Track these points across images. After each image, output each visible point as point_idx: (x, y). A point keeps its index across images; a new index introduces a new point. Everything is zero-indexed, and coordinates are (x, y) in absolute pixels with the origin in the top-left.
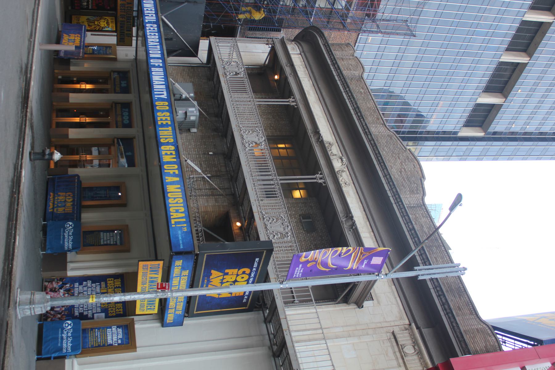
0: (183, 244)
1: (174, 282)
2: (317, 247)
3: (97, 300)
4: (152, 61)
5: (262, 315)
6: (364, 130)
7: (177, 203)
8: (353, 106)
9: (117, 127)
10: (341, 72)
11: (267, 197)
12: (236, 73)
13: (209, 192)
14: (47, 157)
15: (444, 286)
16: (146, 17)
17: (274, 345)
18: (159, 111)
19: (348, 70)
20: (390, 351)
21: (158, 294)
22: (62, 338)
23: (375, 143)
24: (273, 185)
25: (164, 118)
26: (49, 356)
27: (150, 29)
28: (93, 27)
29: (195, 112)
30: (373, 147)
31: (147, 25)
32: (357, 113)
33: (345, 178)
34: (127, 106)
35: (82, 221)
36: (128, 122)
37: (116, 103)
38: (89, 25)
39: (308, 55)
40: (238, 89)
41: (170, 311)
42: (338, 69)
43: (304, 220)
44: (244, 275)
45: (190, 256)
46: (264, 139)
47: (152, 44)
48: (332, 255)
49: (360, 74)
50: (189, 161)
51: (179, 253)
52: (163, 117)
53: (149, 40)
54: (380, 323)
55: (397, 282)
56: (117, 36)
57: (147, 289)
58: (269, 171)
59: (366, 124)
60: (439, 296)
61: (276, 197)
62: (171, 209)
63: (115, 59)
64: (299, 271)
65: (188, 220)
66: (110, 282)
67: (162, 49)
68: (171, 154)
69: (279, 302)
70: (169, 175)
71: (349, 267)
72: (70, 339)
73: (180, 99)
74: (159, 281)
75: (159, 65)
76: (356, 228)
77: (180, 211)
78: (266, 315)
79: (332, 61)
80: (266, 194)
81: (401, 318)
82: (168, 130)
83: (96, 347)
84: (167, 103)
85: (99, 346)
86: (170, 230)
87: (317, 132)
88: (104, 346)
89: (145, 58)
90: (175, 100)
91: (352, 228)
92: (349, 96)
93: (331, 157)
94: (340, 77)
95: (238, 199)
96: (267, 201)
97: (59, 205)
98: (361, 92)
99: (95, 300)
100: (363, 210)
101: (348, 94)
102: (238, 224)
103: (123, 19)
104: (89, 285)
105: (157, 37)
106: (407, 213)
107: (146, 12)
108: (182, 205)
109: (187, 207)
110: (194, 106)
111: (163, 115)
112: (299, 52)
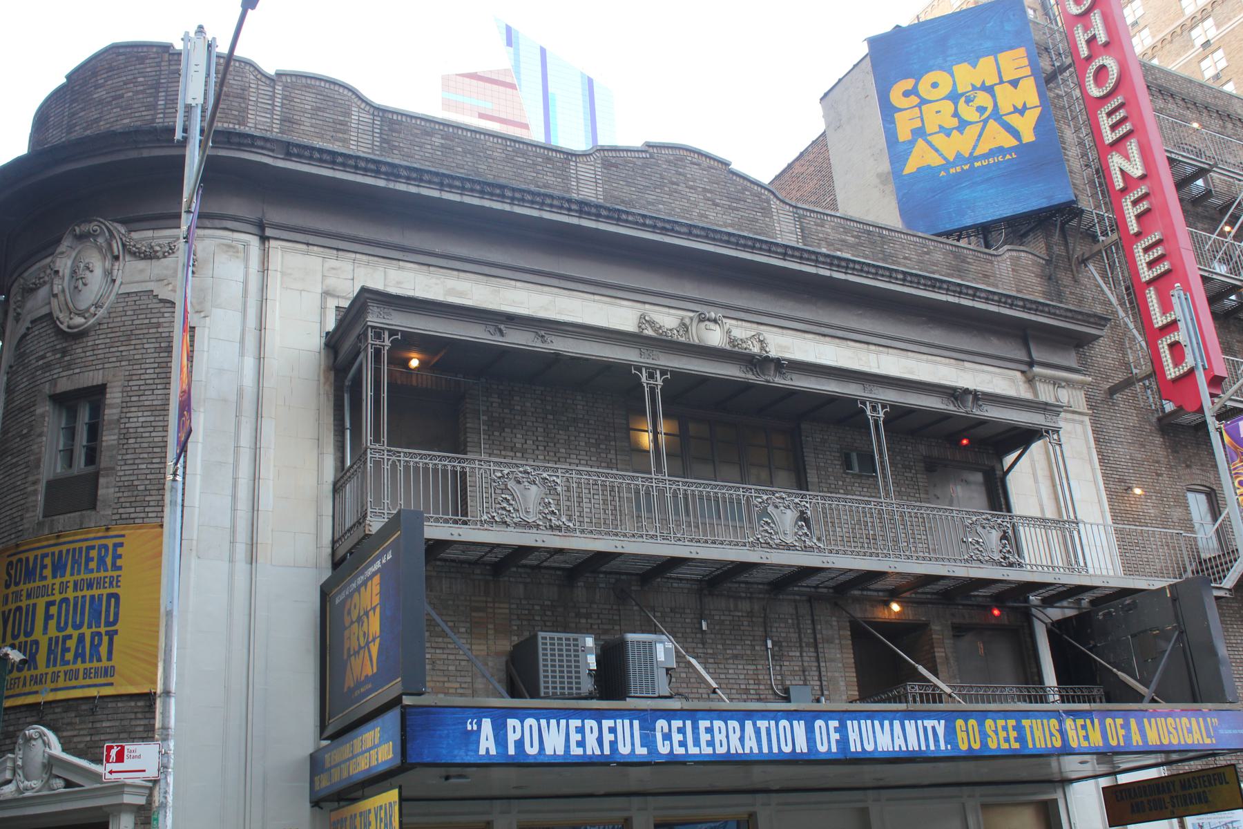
7: (1176, 729)
15: (952, 276)
18: (984, 744)
23: (703, 228)
25: (1002, 734)
30: (707, 237)
53: (735, 747)
60: (1012, 306)
67: (775, 715)
68: (1084, 727)
76: (984, 394)
79: (377, 173)
81: (1012, 380)
82: (1031, 727)
91: (978, 399)
106: (814, 253)
111: (992, 734)
112: (254, 241)
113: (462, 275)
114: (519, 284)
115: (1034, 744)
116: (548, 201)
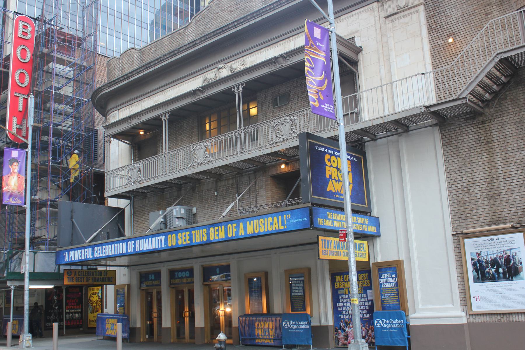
0: (302, 218)
1: (338, 226)
2: (305, 91)
3: (356, 296)
4: (129, 251)
5: (369, 143)
6: (191, 47)
7: (264, 224)
8: (168, 58)
9: (193, 282)
10: (135, 70)
11: (257, 139)
12: (138, 171)
13: (253, 195)
14: (223, 346)
16: (88, 257)
17: (397, 131)
18: (177, 243)
19: (133, 64)
20: (402, 20)
21: (350, 240)
22: (391, 328)
23: (204, 37)
24: (245, 134)
25: (184, 238)
26: (407, 339)
27: (99, 254)
28: (98, 307)
29: (177, 209)
30: (207, 39)
31: (95, 256)
32: (175, 54)
33: (237, 65)
34: (172, 273)
35: (281, 312)
36: (187, 272)
37: (171, 284)
38: (97, 311)
39: (119, 103)
40: (154, 169)
41: (365, 230)
42: (132, 73)
43: (279, 104)
44: (332, 160)
45: (314, 211)
46: (201, 144)
47: (113, 251)
48: (312, 75)
49: (137, 51)
50: (224, 214)
51: (312, 221)
52: (183, 239)
53: (110, 254)
54: (376, 30)
55: (338, 14)
56: (106, 285)
57: (345, 251)
58: (232, 138)
59: (186, 45)
61: (257, 130)
62: (270, 229)
63: (129, 286)
64: (327, 108)
65: (280, 213)
66: (338, 286)
67: (118, 242)
68: (218, 230)
69: (357, 127)
70: (237, 232)
71: (324, 59)
72: (392, 321)
73: (165, 223)
74: (338, 239)
75: (134, 244)
76: (286, 54)
77: (271, 221)
78: (368, 139)
80: (254, 140)
81: (372, 10)
83: (398, 297)
84: (170, 236)
85: (398, 294)
86: (289, 230)
87: (193, 93)
88: (397, 290)
89: (126, 257)
90: (166, 228)
91: (286, 58)
92: (159, 62)
93: (218, 78)
94: (140, 71)
95: (258, 167)
96: (261, 140)
97: (267, 334)
98: (154, 51)
99: (356, 299)
100: (268, 48)
101: (156, 63)
102: (283, 166)
103: (91, 279)
104: (341, 305)
105: (107, 246)
106: (270, 5)
107: (83, 258)
108: (266, 219)
109: (267, 214)
110: (171, 210)
111: (180, 239)
112: (117, 112)
113: (157, 94)
114: (170, 89)
115: (195, 241)
116: (162, 59)
